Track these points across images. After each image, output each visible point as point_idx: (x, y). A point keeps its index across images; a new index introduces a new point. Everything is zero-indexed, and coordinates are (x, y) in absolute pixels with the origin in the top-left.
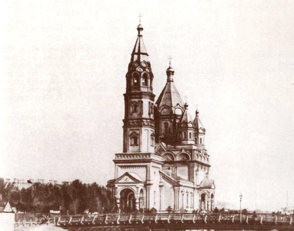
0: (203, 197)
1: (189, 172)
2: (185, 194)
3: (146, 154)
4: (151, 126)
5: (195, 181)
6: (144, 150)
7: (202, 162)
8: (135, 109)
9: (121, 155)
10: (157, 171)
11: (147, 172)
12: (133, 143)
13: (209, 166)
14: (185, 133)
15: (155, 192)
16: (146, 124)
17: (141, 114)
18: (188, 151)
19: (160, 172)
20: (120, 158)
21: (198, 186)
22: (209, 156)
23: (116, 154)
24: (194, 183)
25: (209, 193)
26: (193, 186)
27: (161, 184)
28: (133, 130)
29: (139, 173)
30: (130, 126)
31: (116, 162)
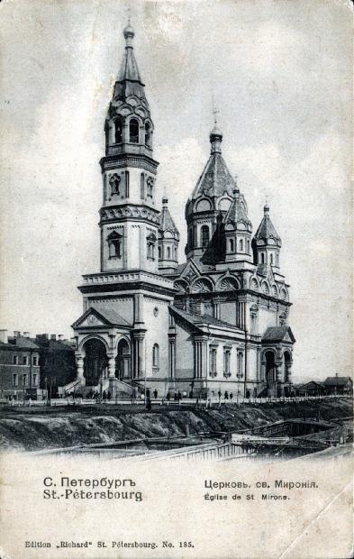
0: (269, 362)
1: (238, 310)
2: (220, 351)
3: (137, 272)
4: (146, 219)
5: (248, 328)
6: (133, 263)
7: (270, 295)
8: (117, 189)
9: (91, 276)
10: (164, 308)
11: (136, 309)
12: (113, 253)
13: (289, 304)
14: (231, 241)
15: (156, 345)
16: (136, 215)
17: (127, 196)
18: (236, 274)
19: (171, 312)
20: (90, 282)
21: (256, 337)
22: (288, 286)
23: (83, 276)
24: (246, 332)
25: (279, 349)
26: (243, 337)
27: (173, 331)
28: (111, 228)
29: (120, 310)
30: (110, 221)
31: (84, 289)
